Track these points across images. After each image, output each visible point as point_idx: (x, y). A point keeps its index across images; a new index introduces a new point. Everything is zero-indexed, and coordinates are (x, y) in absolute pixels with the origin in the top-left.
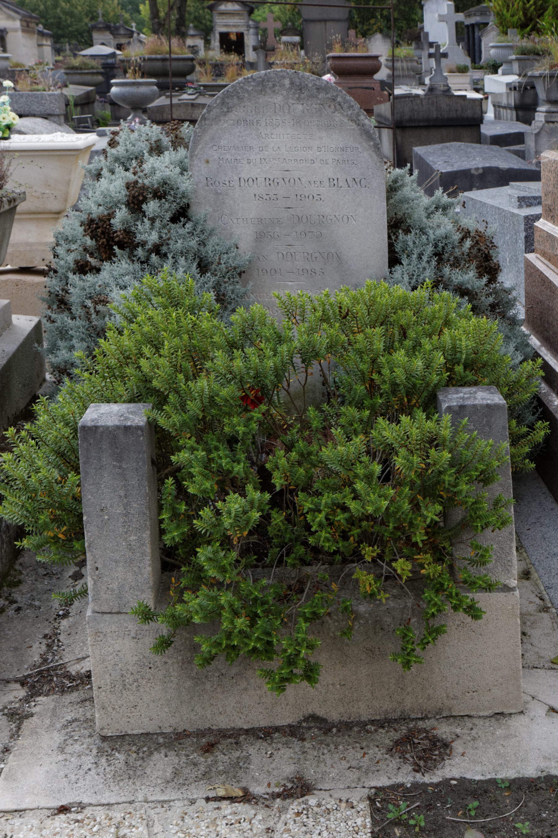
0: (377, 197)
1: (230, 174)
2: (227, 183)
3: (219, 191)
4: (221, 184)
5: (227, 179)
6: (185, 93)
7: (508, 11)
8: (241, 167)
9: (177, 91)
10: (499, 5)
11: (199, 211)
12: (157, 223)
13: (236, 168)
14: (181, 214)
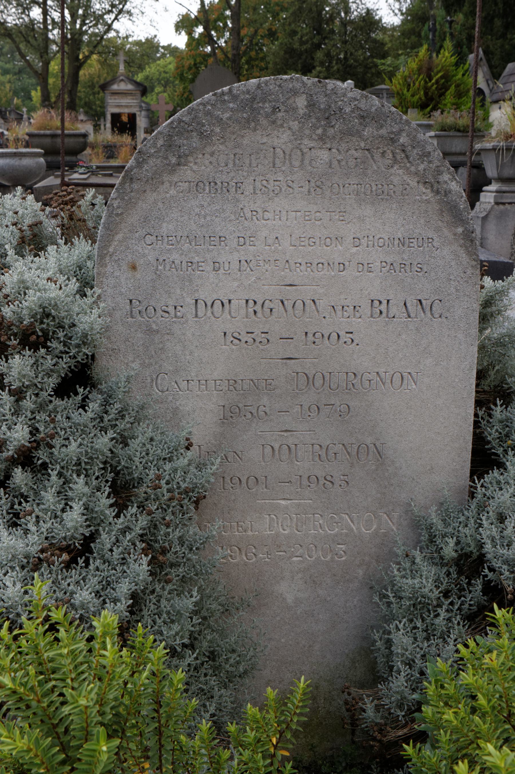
0: (460, 336)
1: (178, 291)
2: (171, 309)
3: (154, 327)
4: (160, 313)
5: (171, 303)
6: (75, 172)
7: (408, 91)
8: (200, 277)
9: (67, 171)
10: (399, 84)
11: (116, 368)
12: (28, 403)
13: (190, 281)
14: (78, 379)
